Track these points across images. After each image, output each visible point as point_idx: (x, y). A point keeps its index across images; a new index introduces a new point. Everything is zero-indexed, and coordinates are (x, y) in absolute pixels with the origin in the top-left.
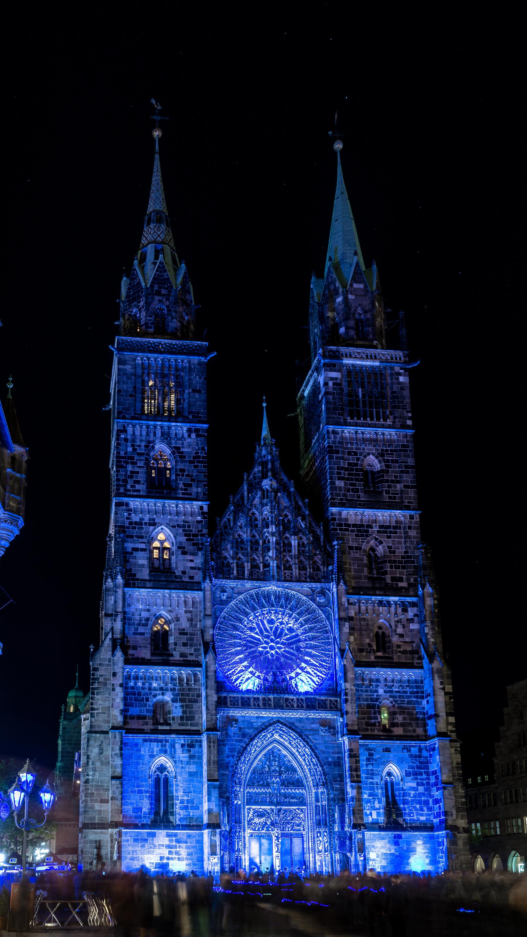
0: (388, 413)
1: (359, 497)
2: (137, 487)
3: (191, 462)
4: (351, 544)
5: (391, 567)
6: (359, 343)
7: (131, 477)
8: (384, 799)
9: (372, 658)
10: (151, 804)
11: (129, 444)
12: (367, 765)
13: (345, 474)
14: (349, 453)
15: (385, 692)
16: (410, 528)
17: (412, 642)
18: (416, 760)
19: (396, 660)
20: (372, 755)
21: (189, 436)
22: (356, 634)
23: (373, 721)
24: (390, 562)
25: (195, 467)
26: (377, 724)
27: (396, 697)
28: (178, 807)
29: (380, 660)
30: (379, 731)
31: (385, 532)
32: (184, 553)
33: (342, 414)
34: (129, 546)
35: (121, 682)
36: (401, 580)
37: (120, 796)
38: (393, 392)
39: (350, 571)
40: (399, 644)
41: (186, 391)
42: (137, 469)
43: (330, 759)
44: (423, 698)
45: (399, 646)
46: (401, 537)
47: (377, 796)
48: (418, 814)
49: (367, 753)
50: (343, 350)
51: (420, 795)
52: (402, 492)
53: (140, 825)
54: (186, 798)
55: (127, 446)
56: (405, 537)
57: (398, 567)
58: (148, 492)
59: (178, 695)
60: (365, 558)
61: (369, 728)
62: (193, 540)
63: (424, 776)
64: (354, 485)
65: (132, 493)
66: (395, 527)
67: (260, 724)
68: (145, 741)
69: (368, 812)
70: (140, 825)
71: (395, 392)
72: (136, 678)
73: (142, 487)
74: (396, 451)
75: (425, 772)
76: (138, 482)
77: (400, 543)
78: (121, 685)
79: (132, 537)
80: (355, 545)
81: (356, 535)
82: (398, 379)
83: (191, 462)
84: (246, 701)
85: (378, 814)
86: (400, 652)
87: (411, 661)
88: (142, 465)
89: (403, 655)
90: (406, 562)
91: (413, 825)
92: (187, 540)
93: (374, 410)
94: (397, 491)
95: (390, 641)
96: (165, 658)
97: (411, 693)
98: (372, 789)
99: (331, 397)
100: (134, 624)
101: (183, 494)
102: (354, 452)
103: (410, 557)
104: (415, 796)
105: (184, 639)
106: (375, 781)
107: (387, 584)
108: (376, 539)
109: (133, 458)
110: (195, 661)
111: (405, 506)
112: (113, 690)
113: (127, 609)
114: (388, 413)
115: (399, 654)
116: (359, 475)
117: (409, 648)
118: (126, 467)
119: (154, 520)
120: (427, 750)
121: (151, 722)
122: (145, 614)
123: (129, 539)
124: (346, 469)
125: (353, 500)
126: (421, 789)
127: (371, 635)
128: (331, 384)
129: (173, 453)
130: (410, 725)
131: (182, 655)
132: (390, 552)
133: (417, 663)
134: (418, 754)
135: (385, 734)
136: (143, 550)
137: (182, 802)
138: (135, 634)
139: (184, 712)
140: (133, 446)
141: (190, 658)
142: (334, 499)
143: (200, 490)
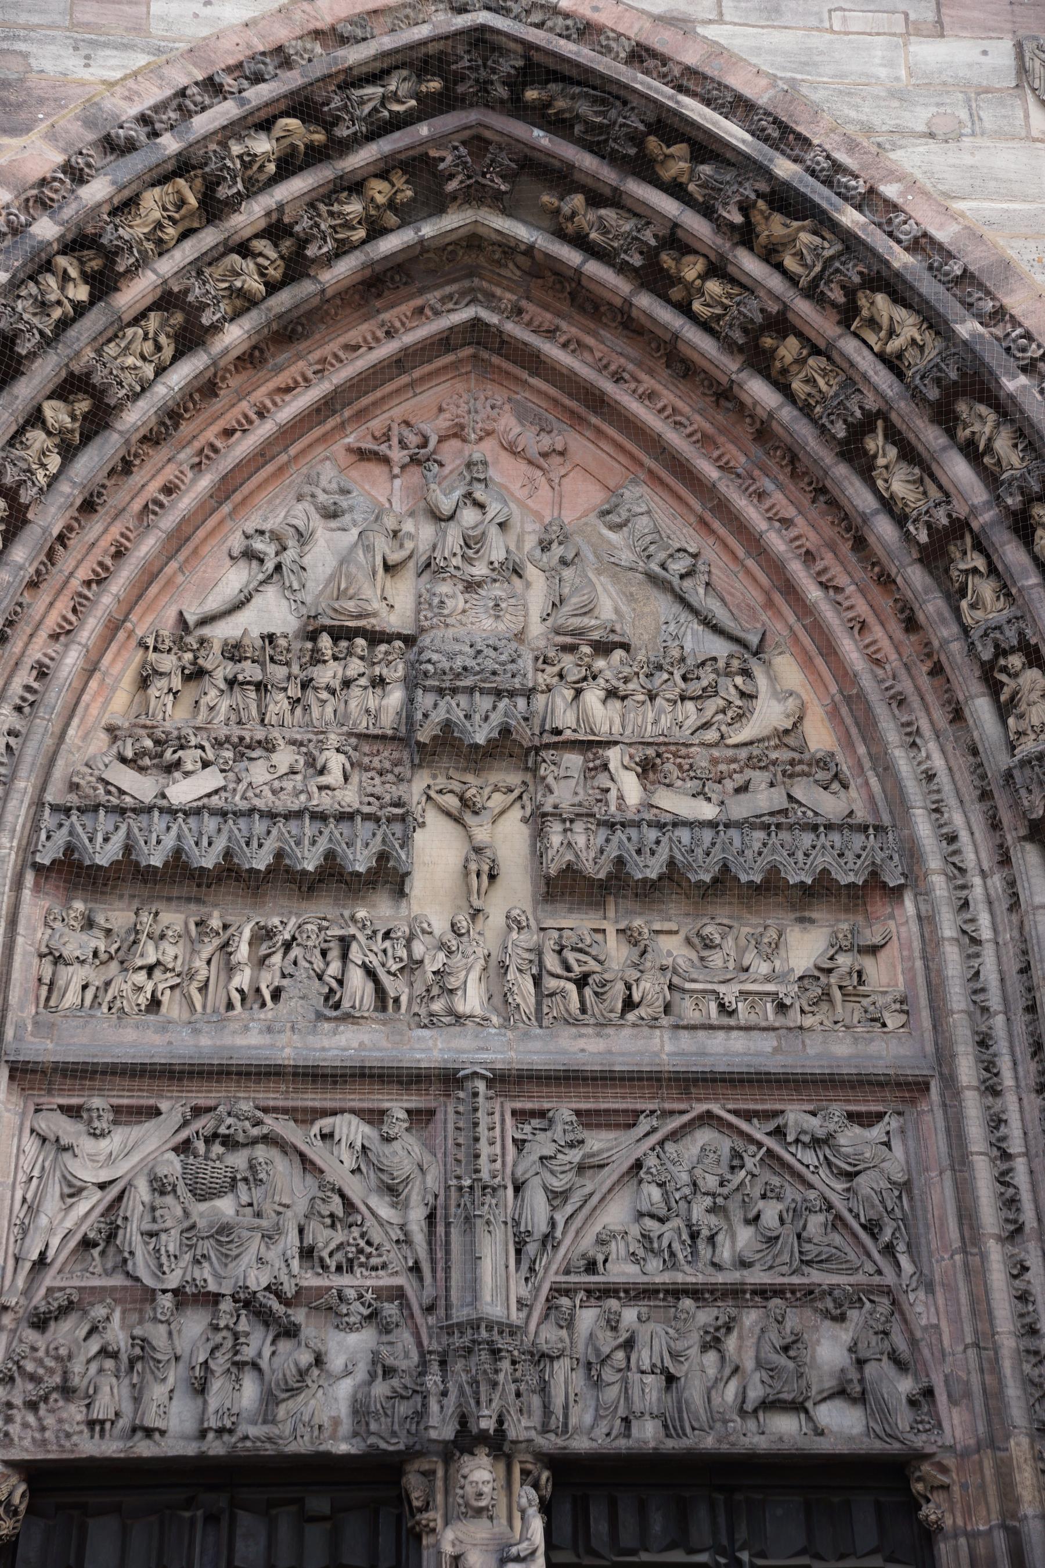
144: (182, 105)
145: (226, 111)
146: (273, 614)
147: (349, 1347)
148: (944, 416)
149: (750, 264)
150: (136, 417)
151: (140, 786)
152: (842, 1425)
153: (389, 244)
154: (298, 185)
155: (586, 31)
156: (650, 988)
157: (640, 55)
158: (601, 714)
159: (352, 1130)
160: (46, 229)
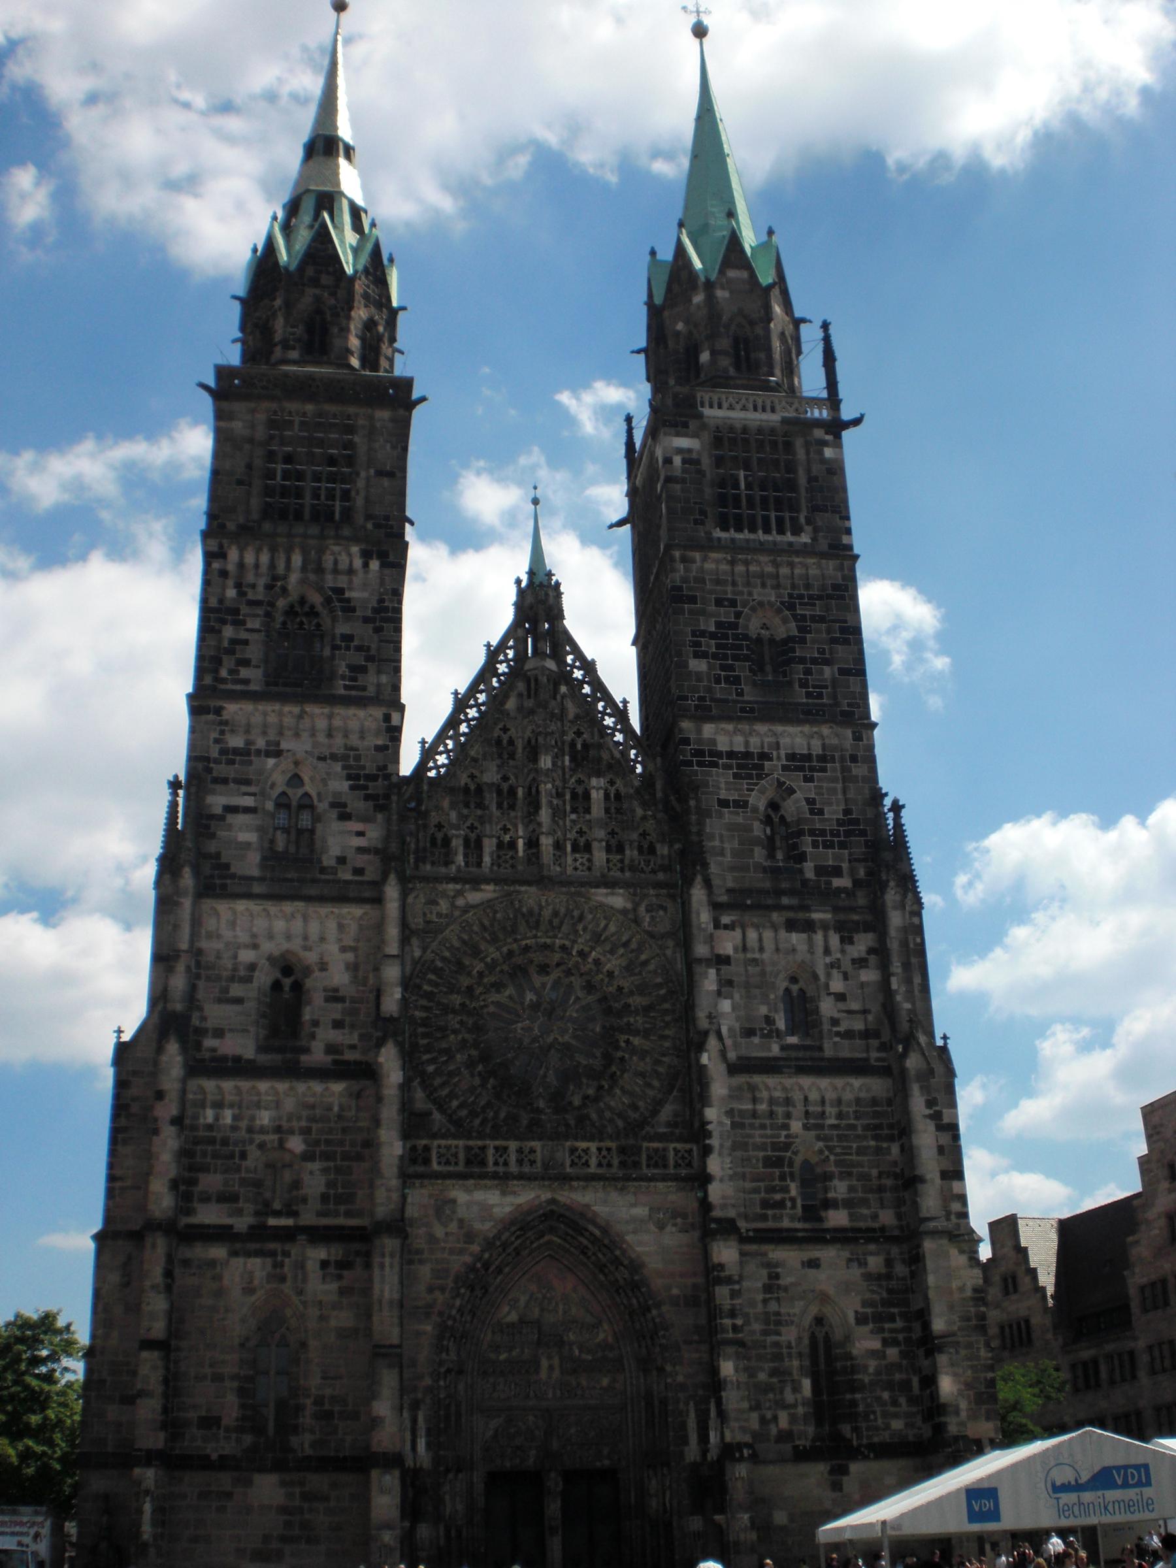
0: (802, 520)
1: (741, 694)
2: (244, 673)
3: (366, 620)
4: (723, 795)
5: (815, 845)
6: (739, 382)
7: (230, 652)
8: (807, 1384)
9: (775, 1050)
10: (243, 1406)
11: (230, 582)
12: (765, 1301)
13: (711, 646)
14: (719, 602)
15: (806, 1127)
16: (854, 759)
17: (865, 1012)
18: (880, 1286)
19: (828, 1052)
20: (778, 1276)
21: (366, 565)
22: (737, 996)
23: (778, 1197)
24: (812, 832)
25: (378, 630)
26: (789, 1204)
27: (831, 1139)
28: (308, 1413)
29: (793, 1054)
30: (792, 1218)
31: (801, 769)
32: (344, 817)
33: (702, 523)
34: (217, 801)
35: (174, 1111)
36: (837, 872)
37: (160, 1389)
38: (811, 479)
39: (722, 854)
40: (836, 1015)
41: (363, 474)
42: (244, 635)
43: (675, 1291)
44: (891, 1139)
45: (835, 1022)
46: (835, 780)
47: (790, 1374)
48: (885, 1415)
49: (765, 1272)
50: (703, 395)
51: (892, 1367)
52: (834, 681)
53: (214, 1456)
54: (328, 1392)
55: (224, 588)
56: (844, 780)
57: (830, 845)
58: (267, 684)
59: (317, 1143)
60: (757, 825)
61: (770, 1212)
62: (366, 788)
63: (899, 1324)
64: (731, 668)
65: (230, 686)
66: (823, 758)
67: (508, 1209)
68: (234, 1254)
69: (769, 1415)
70: (214, 1456)
71: (816, 479)
72: (219, 1105)
73: (254, 675)
74: (820, 598)
75: (902, 1315)
76: (246, 663)
77: (833, 791)
78: (178, 1121)
79: (225, 781)
80: (733, 796)
81: (735, 776)
82: (821, 453)
83: (366, 620)
84: (476, 1155)
85: (793, 1419)
86: (838, 1034)
87: (864, 1055)
88: (257, 625)
89: (846, 1042)
90: (848, 833)
91: (876, 1440)
92: (352, 788)
93: (773, 515)
94: (825, 680)
95: (817, 1011)
96: (289, 1056)
97: (866, 1128)
98: (778, 1357)
99: (678, 487)
100: (219, 978)
101: (346, 687)
102: (728, 599)
103: (856, 822)
104: (878, 1372)
105: (336, 1011)
106: (782, 1339)
107: (805, 882)
108: (780, 784)
109: (236, 611)
110: (361, 1063)
111: (844, 714)
112: (156, 1132)
113: (204, 944)
114: (802, 520)
115: (837, 1039)
116: (740, 647)
117: (858, 1025)
118: (220, 632)
119: (278, 744)
120: (904, 1261)
121: (249, 1208)
122: (247, 956)
123: (218, 787)
124: (713, 636)
125: (726, 701)
126: (893, 1353)
127: (772, 996)
128: (677, 460)
129: (328, 601)
130: (865, 1202)
131: (331, 1049)
132: (812, 812)
133: (878, 1060)
134: (884, 1271)
135: (807, 1226)
136: (248, 810)
137: (319, 1401)
138: (220, 1001)
139: (330, 1184)
140: (238, 586)
141: (349, 1056)
142: (686, 698)
143: (384, 679)
144: (500, 1233)
145: (507, 1234)
146: (513, 1317)
147: (533, 1452)
148: (632, 1290)
149: (600, 1255)
150: (491, 1289)
151: (493, 1356)
152: (607, 1462)
153: (535, 1245)
154: (519, 1241)
155: (569, 1208)
156: (579, 1392)
157: (582, 1215)
158: (572, 1337)
159: (531, 1418)
160: (479, 1265)
